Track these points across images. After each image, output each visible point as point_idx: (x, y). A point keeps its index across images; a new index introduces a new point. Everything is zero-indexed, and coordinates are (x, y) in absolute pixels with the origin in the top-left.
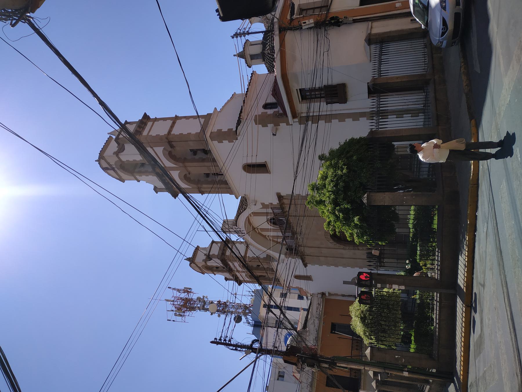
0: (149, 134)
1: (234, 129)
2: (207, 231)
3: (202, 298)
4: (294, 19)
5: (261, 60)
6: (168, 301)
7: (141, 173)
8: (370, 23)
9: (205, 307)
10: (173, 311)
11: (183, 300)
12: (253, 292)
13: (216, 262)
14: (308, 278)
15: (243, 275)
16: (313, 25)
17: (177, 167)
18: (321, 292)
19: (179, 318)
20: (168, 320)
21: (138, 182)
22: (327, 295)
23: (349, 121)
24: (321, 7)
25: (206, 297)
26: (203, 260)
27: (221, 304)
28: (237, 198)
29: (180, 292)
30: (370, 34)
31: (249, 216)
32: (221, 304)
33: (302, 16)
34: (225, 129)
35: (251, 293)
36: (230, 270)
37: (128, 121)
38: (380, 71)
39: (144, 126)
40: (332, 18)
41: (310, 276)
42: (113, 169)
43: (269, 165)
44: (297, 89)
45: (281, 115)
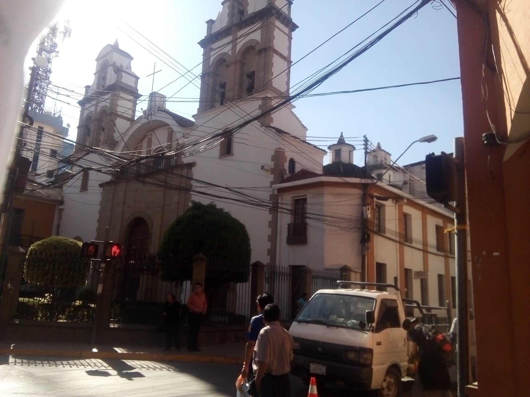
0: (276, 28)
1: (272, 125)
2: (154, 73)
4: (373, 199)
5: (334, 161)
8: (360, 271)
9: (44, 52)
12: (60, 115)
13: (111, 78)
14: (84, 187)
15: (91, 108)
16: (365, 217)
17: (236, 52)
18: (65, 201)
21: (222, 3)
22: (61, 207)
23: (268, 245)
24: (379, 226)
25: (57, 55)
26: (115, 63)
27: (46, 73)
28: (193, 116)
30: (350, 270)
31: (168, 127)
33: (375, 207)
35: (59, 114)
36: (101, 94)
37: (292, 5)
38: (317, 277)
39: (285, 23)
40: (369, 236)
41: (86, 190)
43: (229, 158)
44: (306, 196)
45: (282, 177)
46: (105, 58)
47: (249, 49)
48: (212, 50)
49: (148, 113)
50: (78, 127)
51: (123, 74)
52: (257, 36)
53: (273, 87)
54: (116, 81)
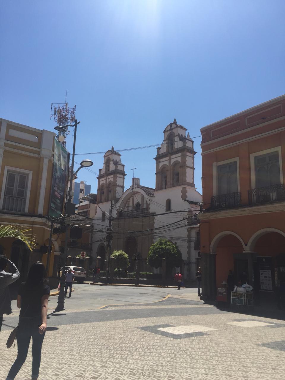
0: (187, 156)
1: (187, 199)
3: (68, 130)
6: (66, 105)
7: (168, 143)
10: (59, 108)
11: (66, 115)
13: (112, 167)
15: (103, 181)
19: (53, 113)
20: (52, 104)
23: (187, 250)
26: (113, 159)
29: (71, 113)
32: (63, 144)
34: (187, 194)
37: (194, 143)
42: (170, 130)
46: (108, 157)
47: (176, 163)
48: (160, 162)
49: (133, 187)
50: (98, 190)
51: (118, 165)
52: (179, 159)
53: (187, 182)
54: (115, 170)
